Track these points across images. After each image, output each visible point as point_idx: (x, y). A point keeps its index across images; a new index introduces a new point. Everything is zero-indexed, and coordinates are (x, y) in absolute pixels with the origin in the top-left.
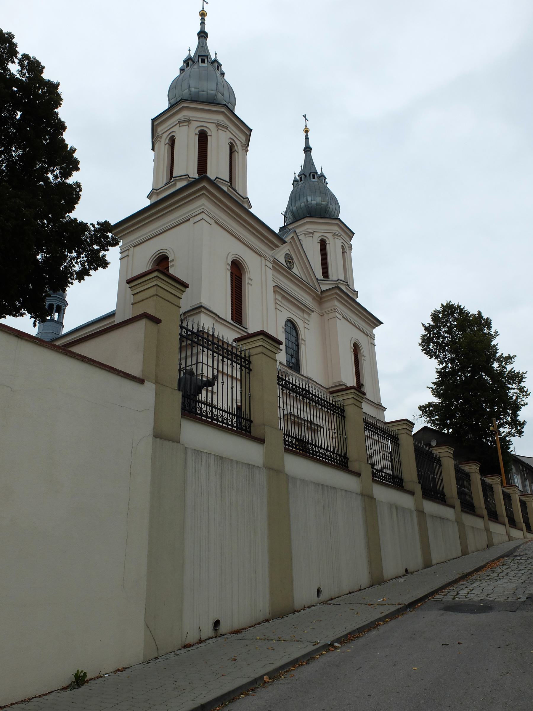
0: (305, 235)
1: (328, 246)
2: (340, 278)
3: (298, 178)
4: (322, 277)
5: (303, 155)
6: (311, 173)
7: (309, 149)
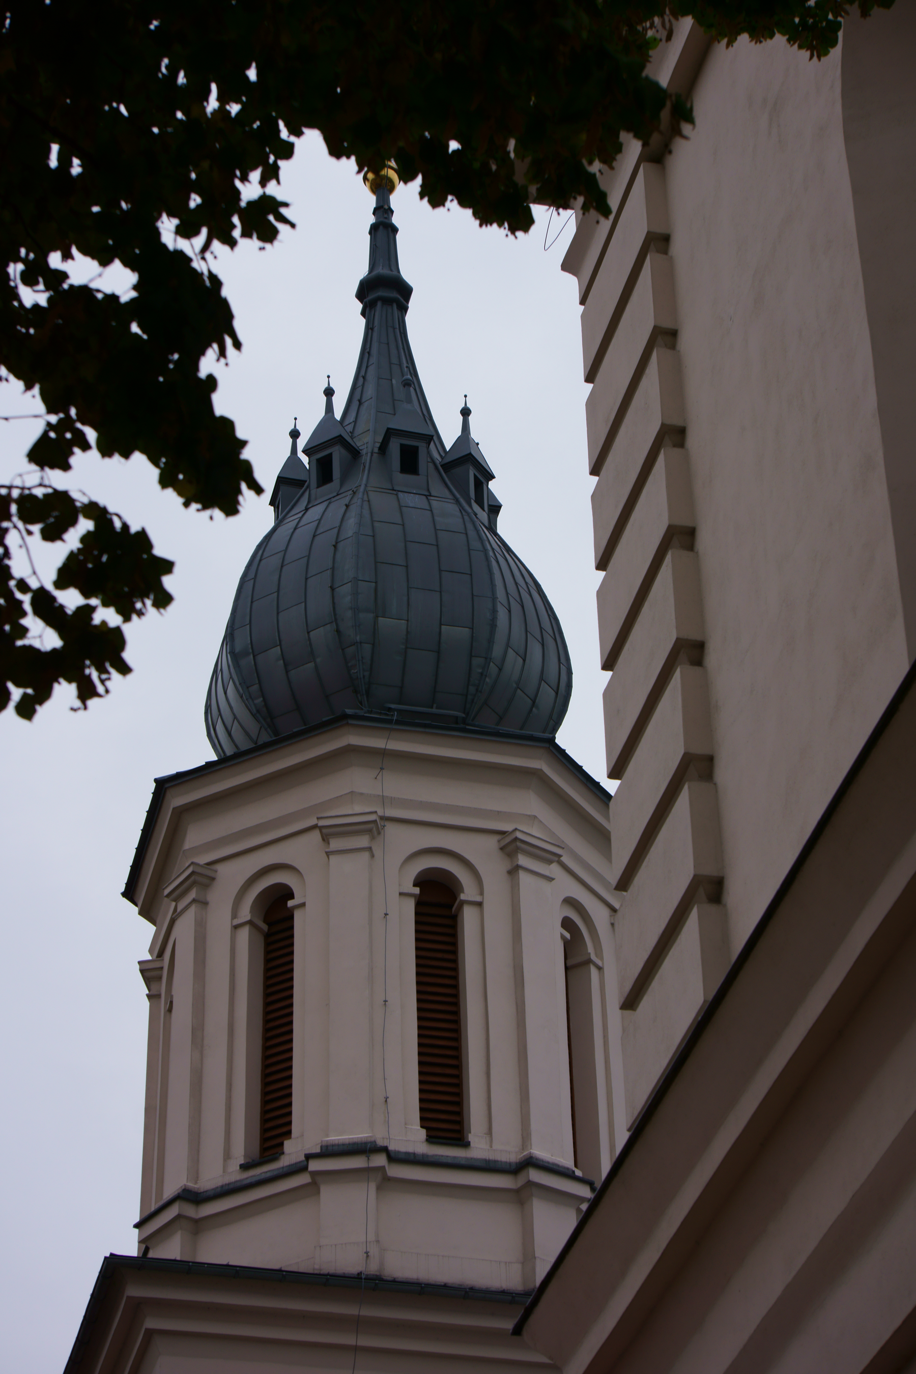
0: (325, 839)
1: (469, 917)
2: (540, 1152)
3: (305, 459)
4: (410, 1136)
5: (350, 326)
6: (390, 433)
7: (394, 295)
